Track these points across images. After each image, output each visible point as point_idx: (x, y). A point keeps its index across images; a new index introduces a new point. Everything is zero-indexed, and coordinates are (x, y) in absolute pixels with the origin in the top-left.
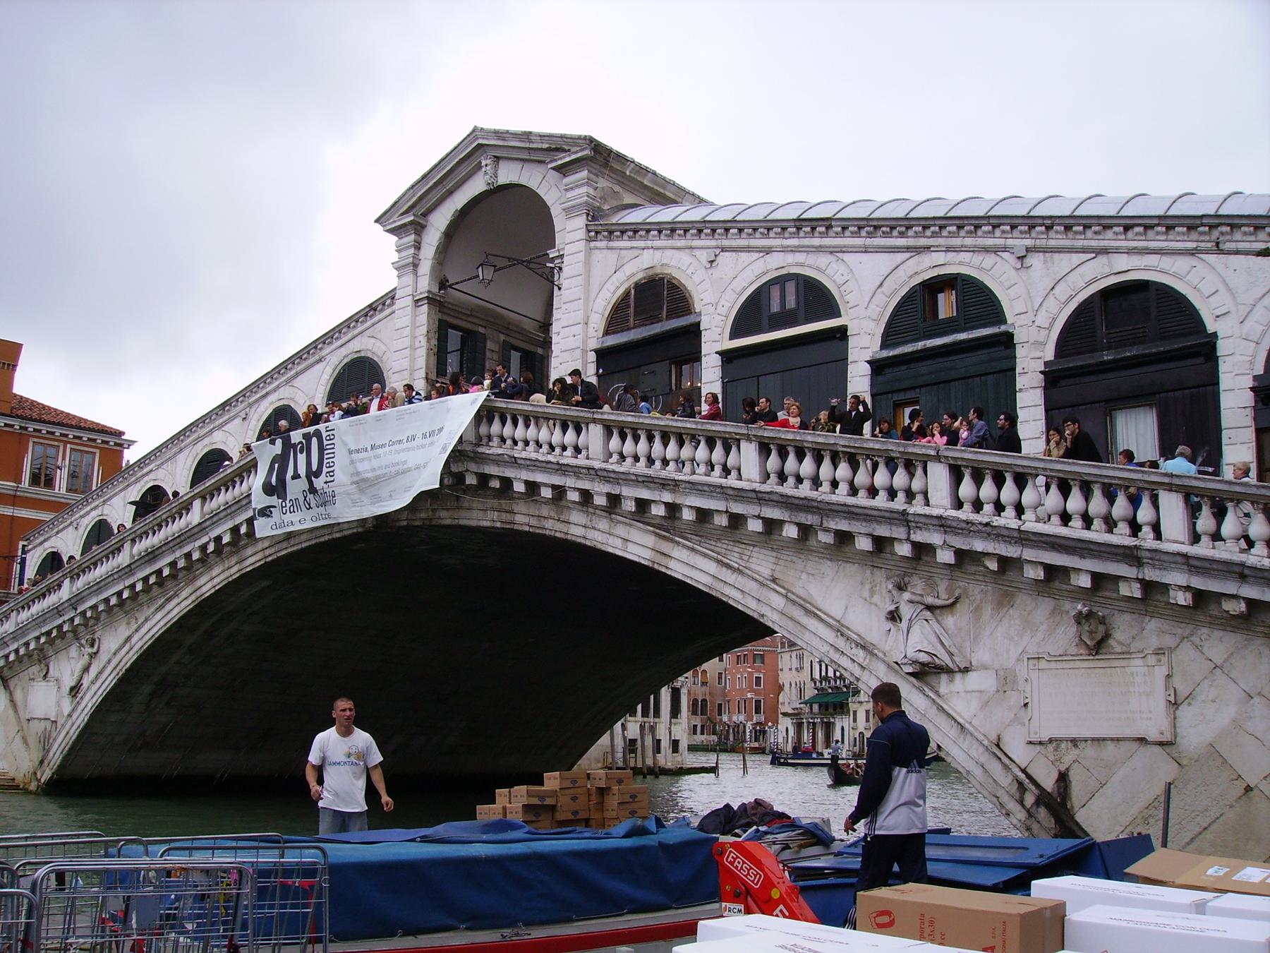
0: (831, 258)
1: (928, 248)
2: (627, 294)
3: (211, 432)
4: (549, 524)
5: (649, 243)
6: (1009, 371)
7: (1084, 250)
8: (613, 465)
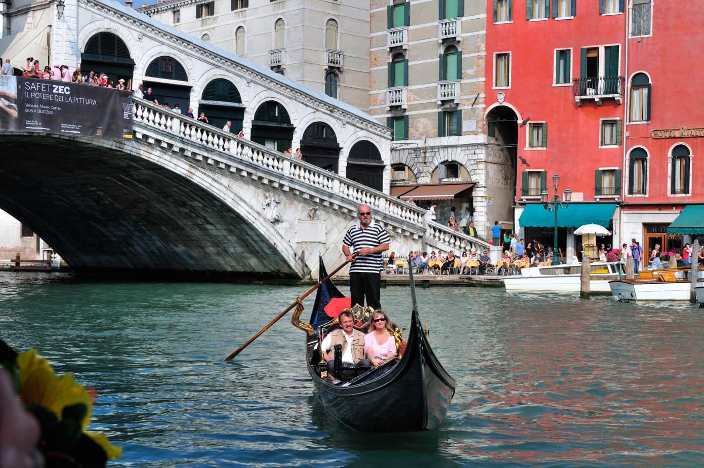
0: (187, 57)
1: (220, 67)
4: (142, 152)
5: (109, 17)
7: (265, 87)
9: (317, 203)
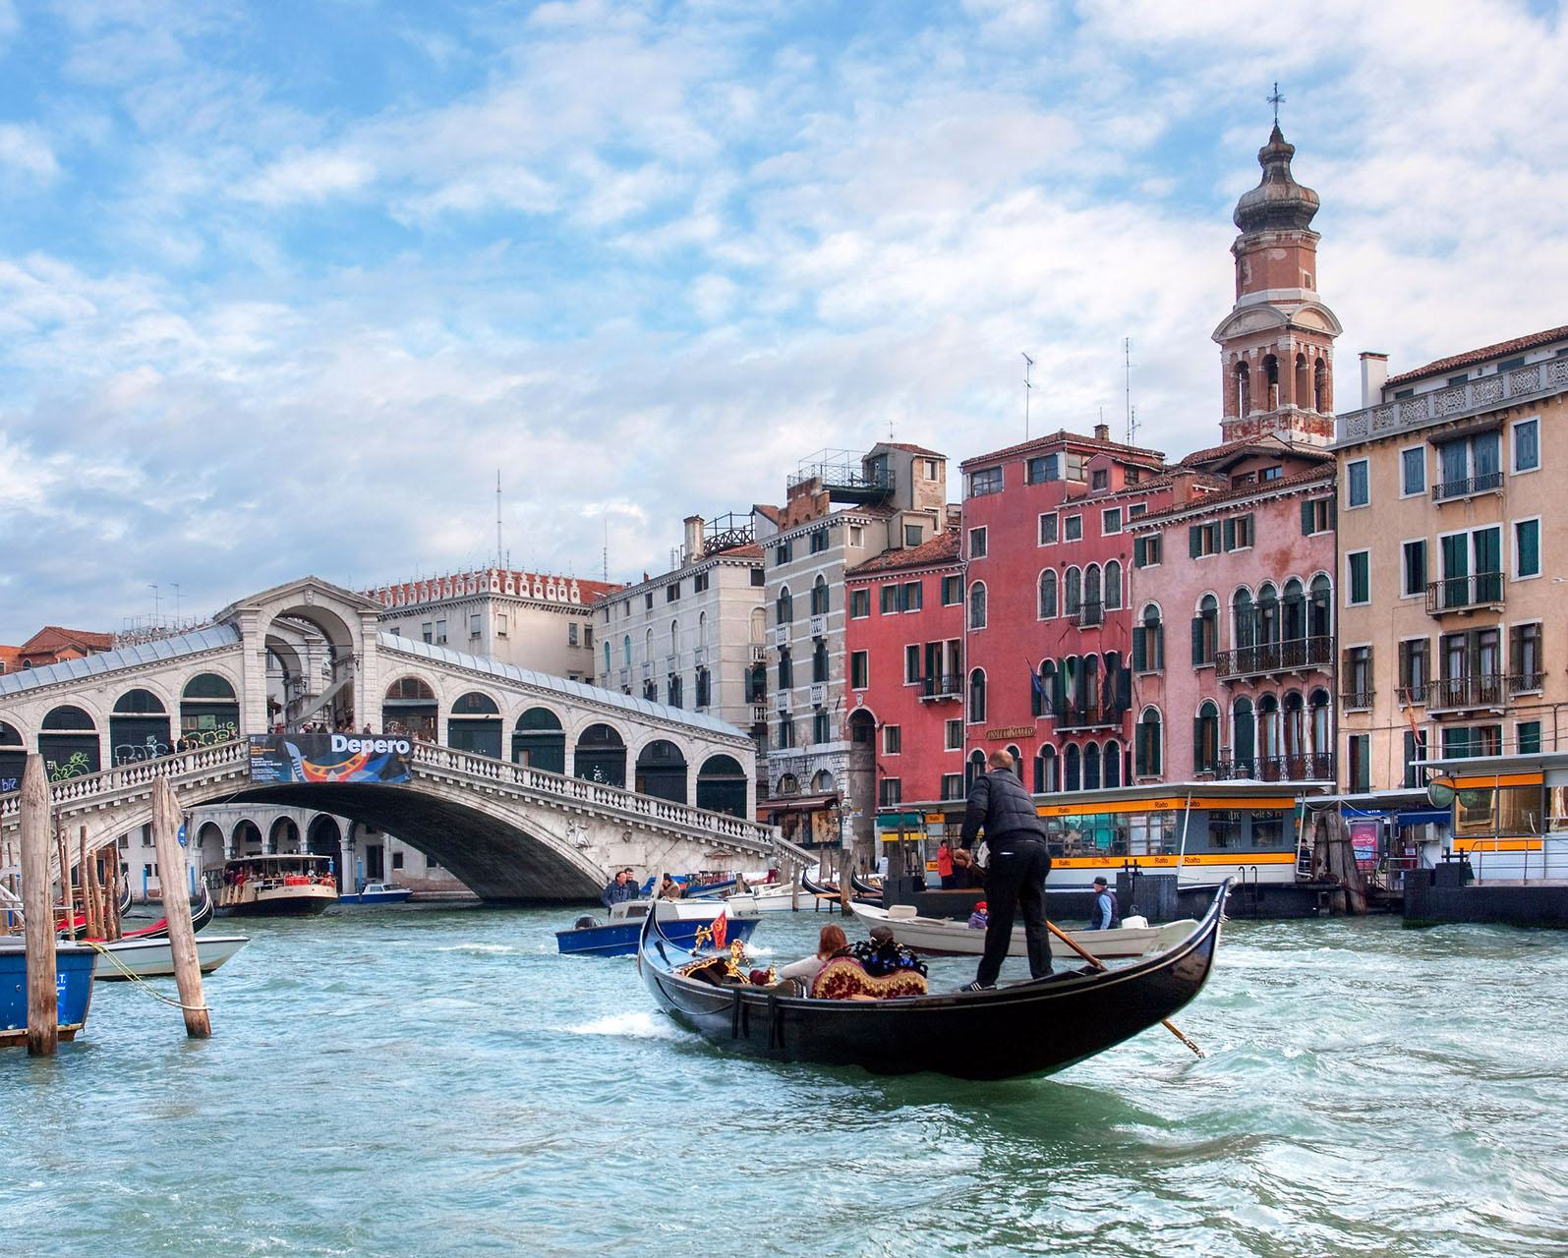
2: (398, 681)
3: (64, 694)
6: (563, 746)
8: (469, 772)
9: (629, 828)
